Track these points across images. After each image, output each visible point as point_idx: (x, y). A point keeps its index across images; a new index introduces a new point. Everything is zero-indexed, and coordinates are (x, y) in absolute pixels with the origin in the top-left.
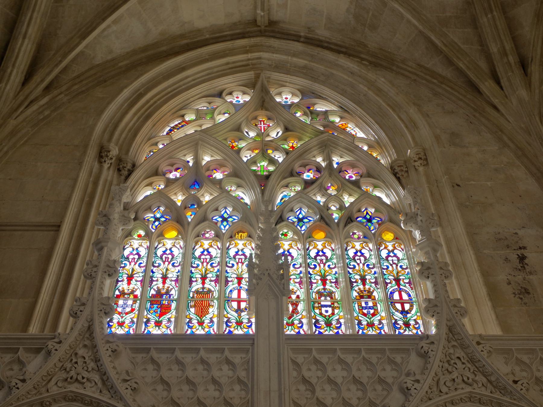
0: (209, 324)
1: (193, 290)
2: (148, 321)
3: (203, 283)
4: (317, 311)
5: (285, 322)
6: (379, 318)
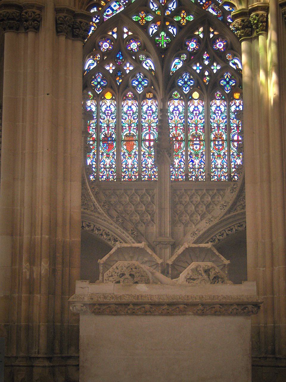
0: (134, 156)
1: (124, 134)
2: (102, 154)
3: (130, 130)
4: (192, 148)
5: (174, 154)
6: (224, 151)
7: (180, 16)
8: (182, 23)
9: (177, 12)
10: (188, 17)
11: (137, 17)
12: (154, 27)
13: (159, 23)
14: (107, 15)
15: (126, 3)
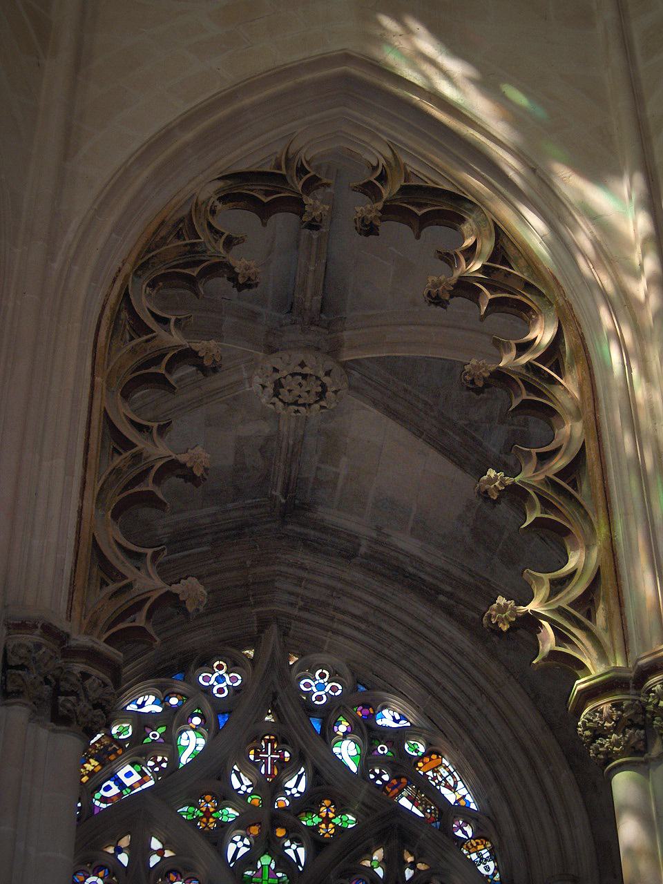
7: (318, 814)
8: (324, 834)
9: (308, 803)
10: (341, 819)
11: (191, 809)
12: (242, 840)
13: (255, 830)
14: (103, 799)
15: (161, 768)
